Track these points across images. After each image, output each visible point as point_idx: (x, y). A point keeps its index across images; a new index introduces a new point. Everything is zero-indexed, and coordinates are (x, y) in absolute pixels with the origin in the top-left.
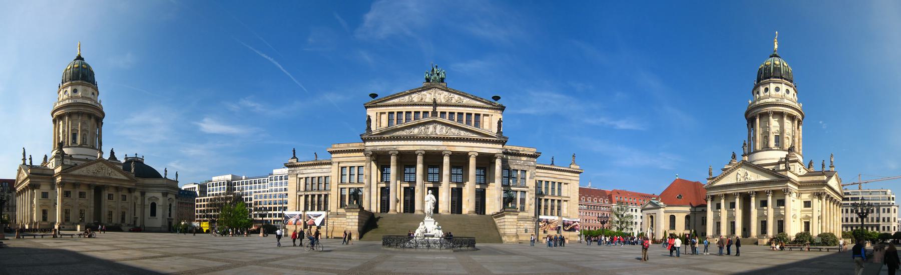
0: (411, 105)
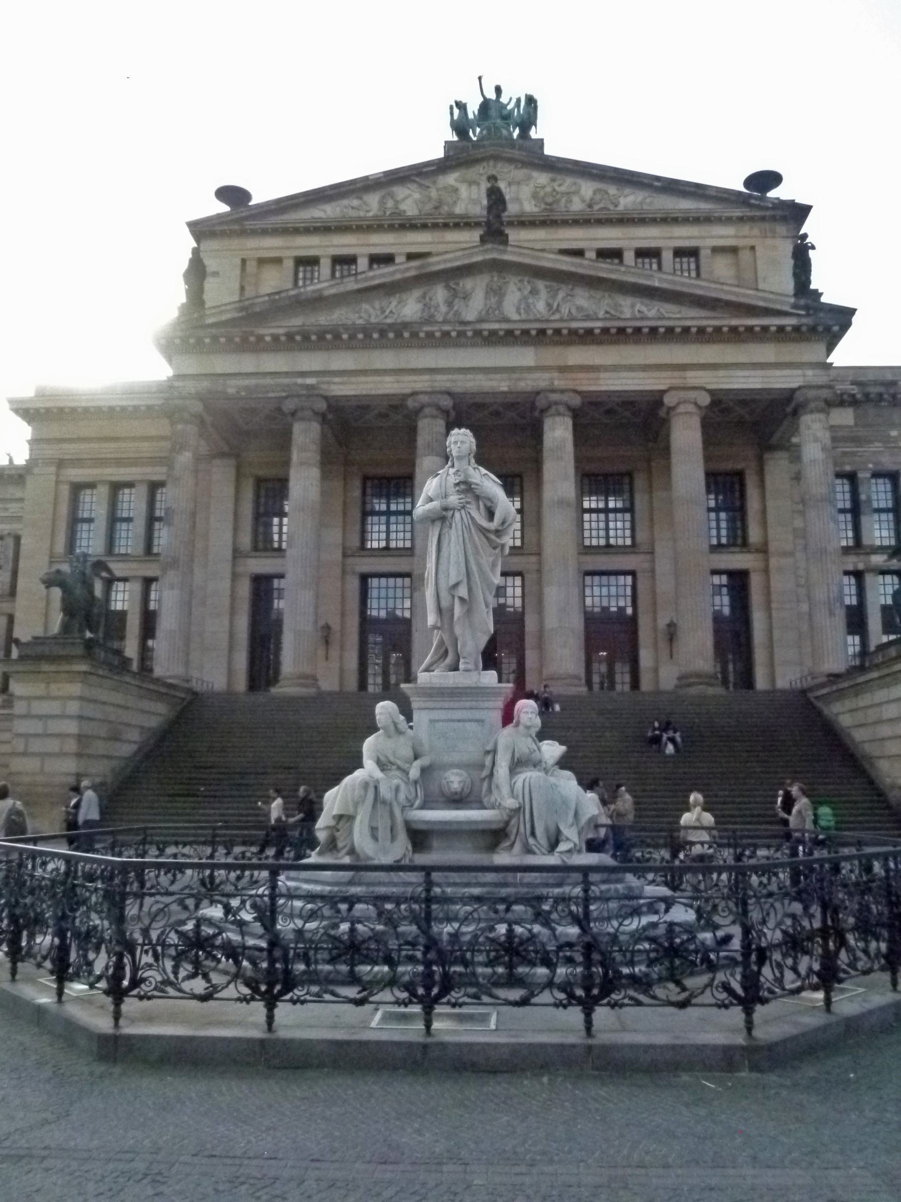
0: (391, 228)
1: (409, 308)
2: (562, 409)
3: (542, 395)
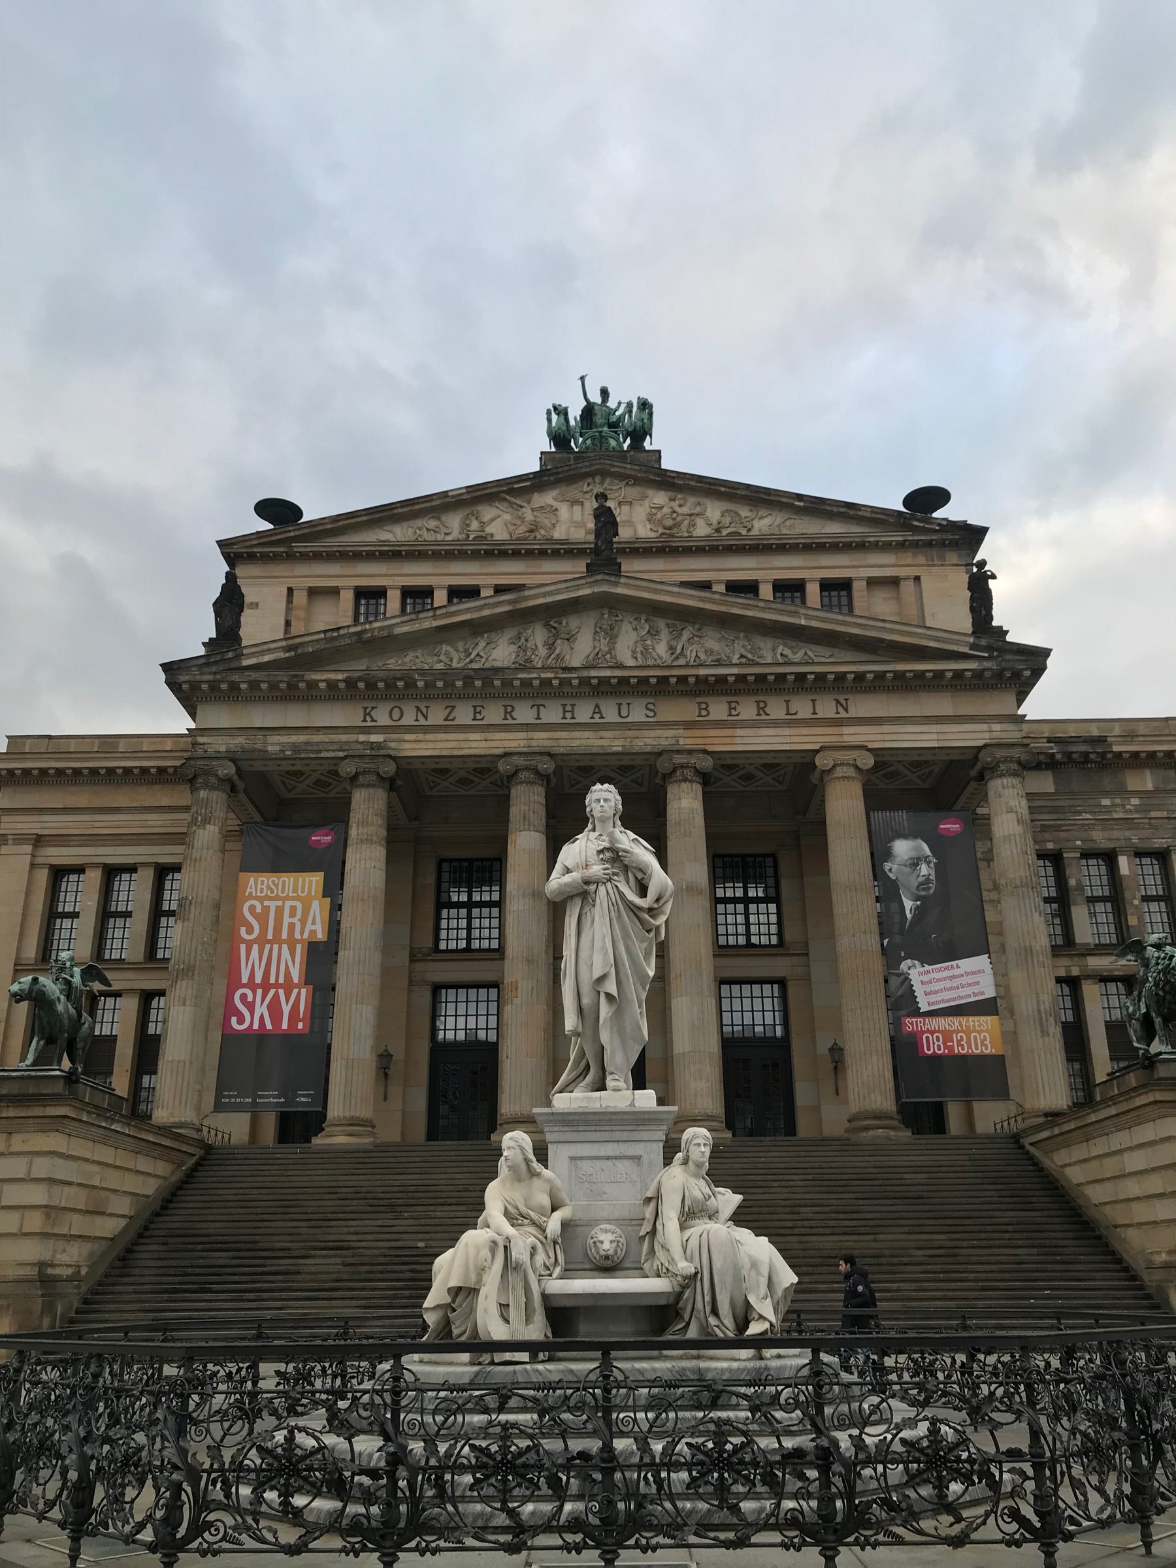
0: (476, 555)
1: (502, 653)
2: (689, 773)
3: (664, 756)
